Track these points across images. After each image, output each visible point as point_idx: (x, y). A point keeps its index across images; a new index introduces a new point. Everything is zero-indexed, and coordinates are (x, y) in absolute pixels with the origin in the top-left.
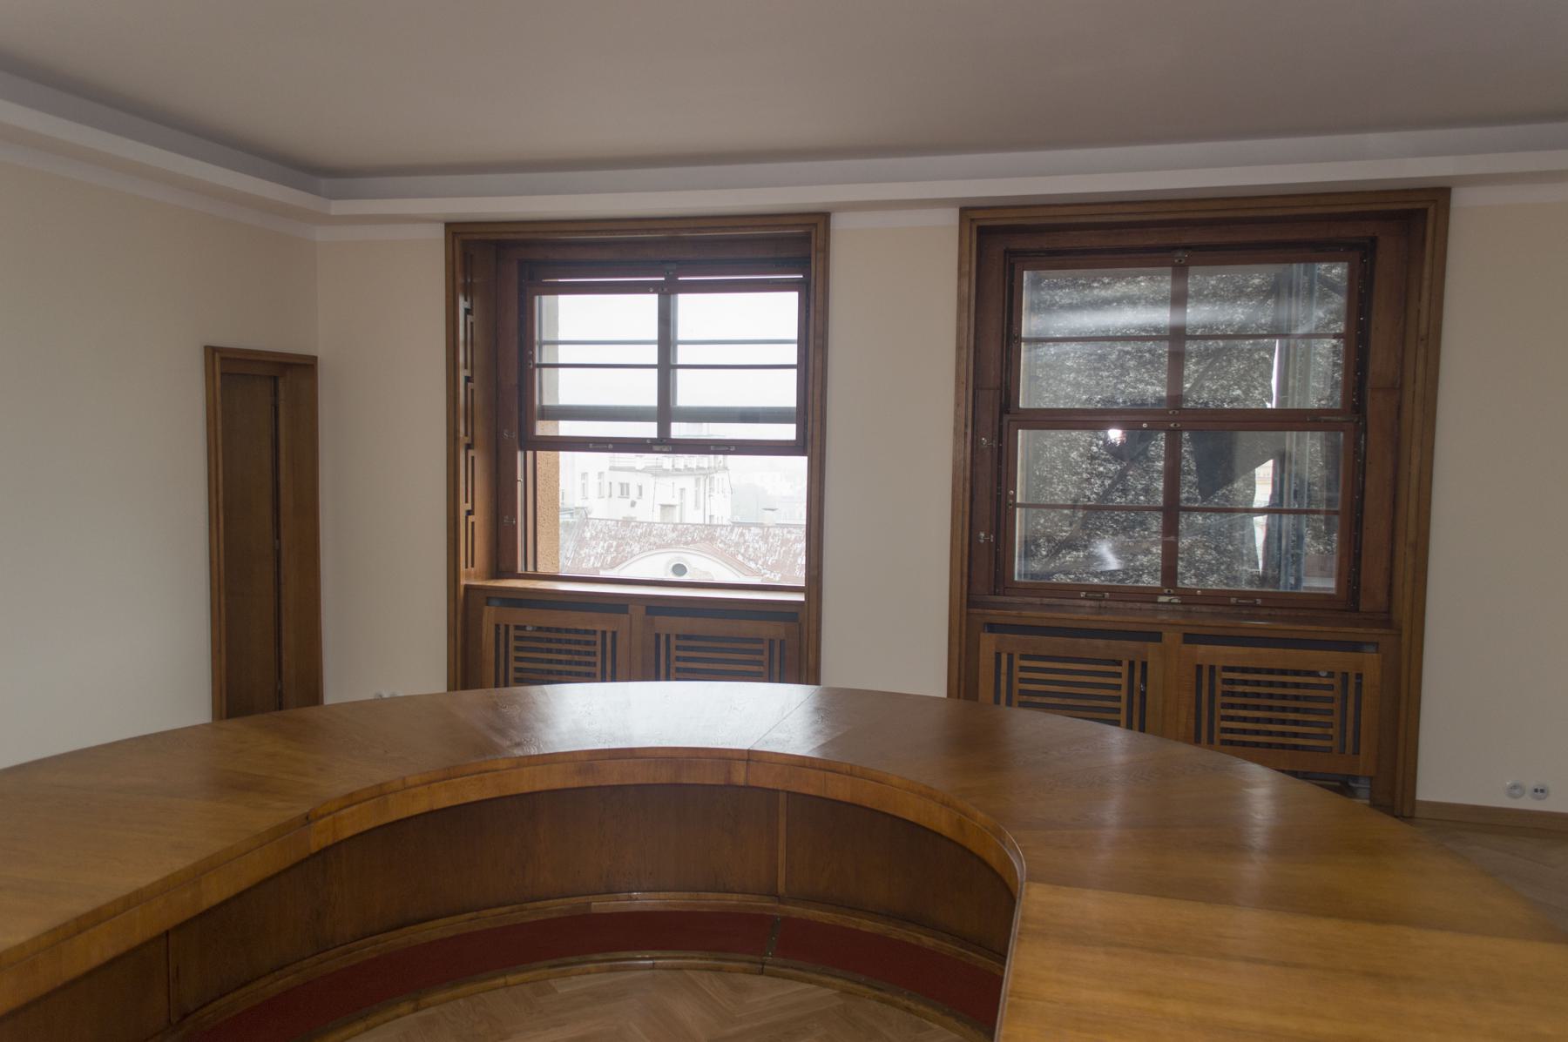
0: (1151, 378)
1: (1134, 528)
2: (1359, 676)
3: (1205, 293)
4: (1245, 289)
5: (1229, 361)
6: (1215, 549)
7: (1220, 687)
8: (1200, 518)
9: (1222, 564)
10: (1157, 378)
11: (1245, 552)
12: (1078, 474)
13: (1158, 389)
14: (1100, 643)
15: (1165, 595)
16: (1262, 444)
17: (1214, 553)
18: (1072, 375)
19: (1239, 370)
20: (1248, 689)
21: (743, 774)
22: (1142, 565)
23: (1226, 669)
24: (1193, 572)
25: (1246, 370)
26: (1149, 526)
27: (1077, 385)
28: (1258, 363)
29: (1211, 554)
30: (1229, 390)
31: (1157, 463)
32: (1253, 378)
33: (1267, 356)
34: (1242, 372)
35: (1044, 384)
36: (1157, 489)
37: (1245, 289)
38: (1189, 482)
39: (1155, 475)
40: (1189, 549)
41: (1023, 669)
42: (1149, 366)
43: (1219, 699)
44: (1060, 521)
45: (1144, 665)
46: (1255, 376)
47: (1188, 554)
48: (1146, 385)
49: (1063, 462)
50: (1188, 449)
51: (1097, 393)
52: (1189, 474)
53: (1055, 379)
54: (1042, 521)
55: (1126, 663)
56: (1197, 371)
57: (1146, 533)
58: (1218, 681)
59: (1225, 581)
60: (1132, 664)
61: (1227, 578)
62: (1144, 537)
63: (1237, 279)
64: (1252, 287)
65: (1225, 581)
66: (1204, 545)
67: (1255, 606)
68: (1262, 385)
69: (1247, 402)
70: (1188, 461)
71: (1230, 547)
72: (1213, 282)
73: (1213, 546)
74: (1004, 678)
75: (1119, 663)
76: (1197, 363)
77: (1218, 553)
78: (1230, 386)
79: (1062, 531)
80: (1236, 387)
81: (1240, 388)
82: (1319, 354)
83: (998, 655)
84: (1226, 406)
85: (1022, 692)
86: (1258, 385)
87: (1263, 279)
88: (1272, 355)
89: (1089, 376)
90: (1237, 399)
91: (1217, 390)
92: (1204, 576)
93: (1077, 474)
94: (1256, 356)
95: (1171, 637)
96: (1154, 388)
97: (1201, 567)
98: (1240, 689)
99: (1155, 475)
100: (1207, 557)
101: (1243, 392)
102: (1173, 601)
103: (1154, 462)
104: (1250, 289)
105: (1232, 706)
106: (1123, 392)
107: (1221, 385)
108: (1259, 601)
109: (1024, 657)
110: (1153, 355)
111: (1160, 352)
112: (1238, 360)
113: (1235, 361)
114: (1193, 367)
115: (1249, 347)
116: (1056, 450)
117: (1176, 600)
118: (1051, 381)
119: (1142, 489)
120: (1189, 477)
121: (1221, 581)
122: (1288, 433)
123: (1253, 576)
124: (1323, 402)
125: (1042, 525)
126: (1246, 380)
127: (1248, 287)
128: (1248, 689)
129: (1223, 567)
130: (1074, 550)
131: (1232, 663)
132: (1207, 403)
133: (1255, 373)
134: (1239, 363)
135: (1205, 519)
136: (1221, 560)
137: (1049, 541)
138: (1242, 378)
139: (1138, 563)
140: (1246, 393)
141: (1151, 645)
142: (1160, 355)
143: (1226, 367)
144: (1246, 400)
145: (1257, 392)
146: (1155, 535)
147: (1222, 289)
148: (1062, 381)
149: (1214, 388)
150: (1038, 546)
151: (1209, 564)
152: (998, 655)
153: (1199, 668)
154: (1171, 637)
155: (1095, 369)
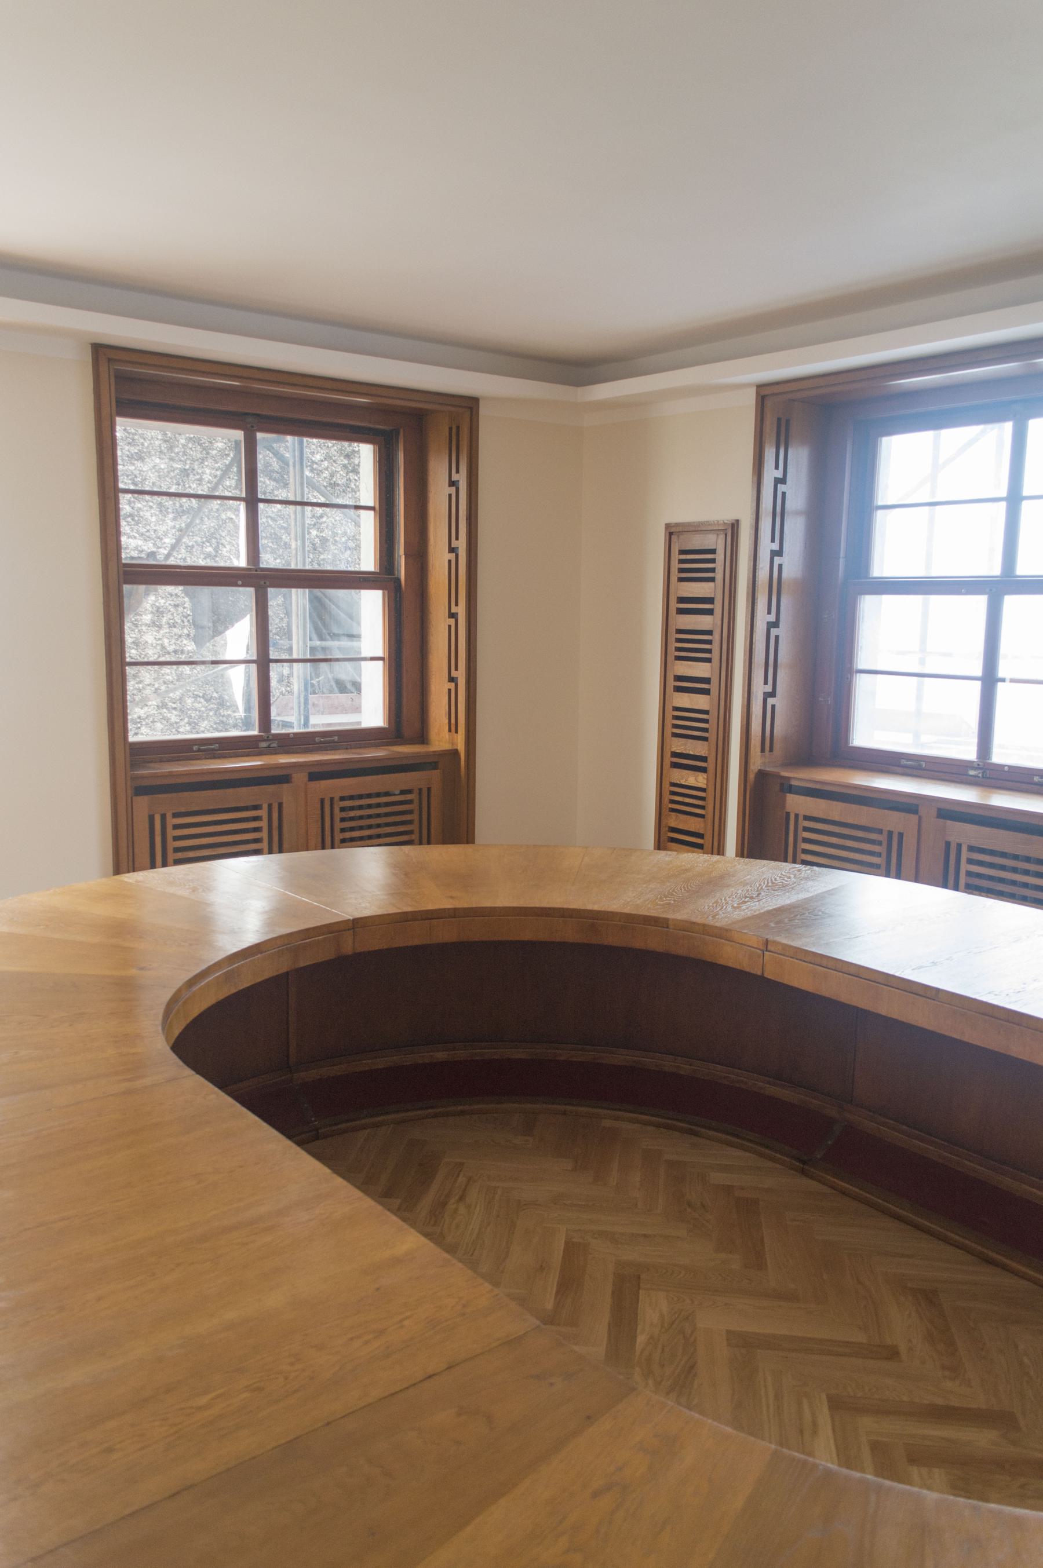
0: (132, 531)
2: (429, 789)
3: (176, 450)
4: (210, 451)
5: (202, 519)
6: (203, 697)
7: (338, 815)
8: (188, 669)
9: (210, 710)
10: (138, 532)
11: (226, 697)
13: (140, 543)
14: (243, 790)
15: (264, 740)
16: (244, 598)
17: (202, 700)
20: (358, 813)
21: (350, 942)
22: (139, 717)
23: (342, 799)
24: (186, 720)
25: (215, 529)
26: (142, 679)
28: (225, 522)
29: (200, 702)
30: (202, 547)
31: (144, 617)
32: (221, 536)
33: (234, 517)
34: (212, 530)
36: (147, 642)
37: (210, 451)
38: (175, 635)
39: (144, 628)
40: (181, 699)
41: (176, 827)
42: (129, 519)
43: (338, 825)
45: (280, 805)
46: (223, 534)
47: (180, 703)
48: (129, 538)
50: (172, 603)
52: (175, 627)
55: (265, 806)
56: (174, 527)
57: (141, 686)
58: (337, 810)
59: (215, 726)
60: (270, 806)
61: (216, 723)
62: (139, 690)
63: (203, 441)
64: (216, 449)
65: (215, 726)
66: (193, 694)
67: (334, 742)
68: (230, 543)
69: (217, 559)
70: (172, 614)
71: (215, 695)
72: (183, 441)
73: (201, 695)
74: (158, 839)
75: (256, 807)
76: (174, 519)
77: (207, 701)
78: (203, 543)
80: (208, 544)
81: (211, 545)
82: (269, 516)
83: (151, 818)
84: (201, 562)
85: (177, 850)
86: (226, 543)
87: (225, 443)
88: (238, 516)
90: (208, 556)
91: (193, 547)
92: (196, 724)
94: (224, 516)
95: (300, 778)
96: (135, 541)
97: (193, 715)
98: (352, 814)
99: (144, 628)
100: (197, 705)
101: (214, 549)
102: (272, 746)
103: (141, 615)
104: (214, 452)
105: (352, 829)
107: (196, 542)
108: (336, 738)
109: (175, 815)
110: (133, 508)
111: (139, 505)
112: (209, 519)
113: (206, 519)
114: (170, 524)
115: (217, 507)
117: (274, 745)
119: (133, 642)
120: (175, 629)
121: (211, 727)
122: (294, 590)
123: (236, 720)
124: (278, 561)
126: (216, 538)
127: (213, 449)
128: (358, 813)
129: (211, 713)
131: (346, 794)
132: (185, 559)
133: (223, 531)
134: (210, 521)
135: (191, 670)
136: (209, 707)
138: (212, 536)
139: (135, 716)
140: (216, 549)
141: (285, 786)
142: (140, 509)
143: (199, 524)
144: (216, 556)
145: (225, 549)
146: (149, 687)
147: (191, 449)
149: (190, 544)
151: (200, 711)
152: (151, 818)
153: (322, 801)
154: (300, 778)
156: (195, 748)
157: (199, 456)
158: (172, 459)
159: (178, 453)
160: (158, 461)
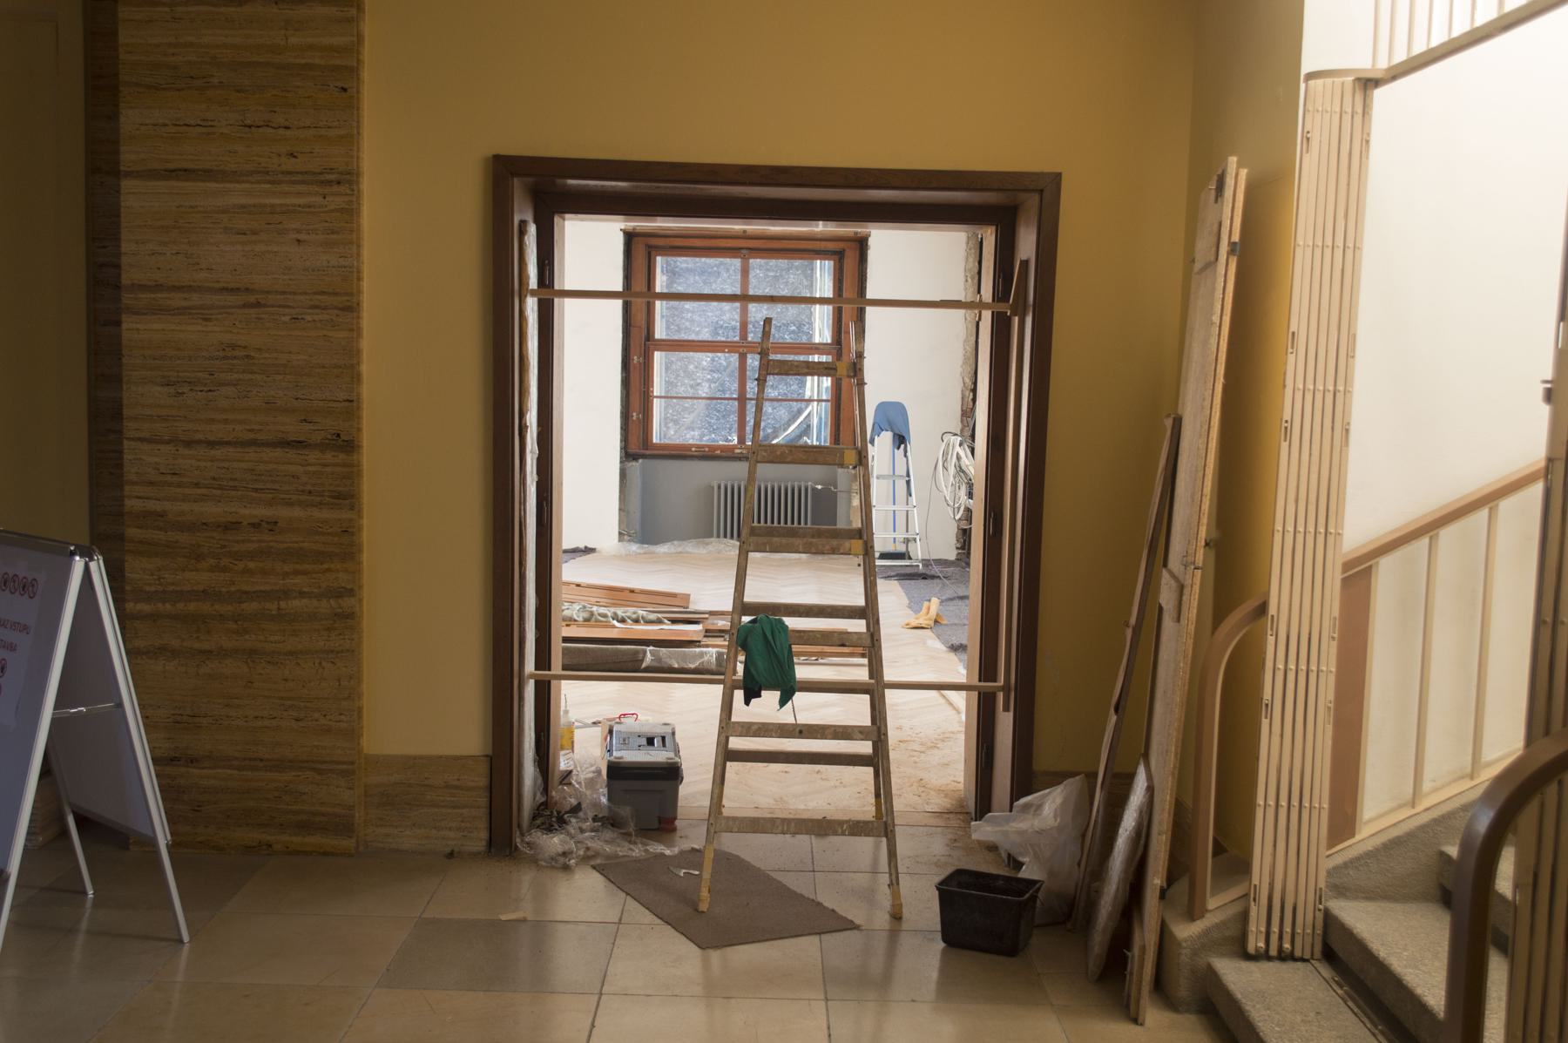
1: (729, 415)
12: (693, 380)
18: (690, 315)
19: (793, 314)
27: (692, 321)
35: (671, 320)
44: (683, 411)
49: (684, 372)
51: (706, 327)
53: (678, 316)
54: (671, 411)
79: (684, 418)
89: (700, 316)
90: (793, 332)
93: (693, 380)
106: (722, 327)
107: (783, 324)
116: (680, 364)
118: (675, 318)
125: (671, 414)
130: (693, 430)
137: (676, 425)
148: (683, 318)
150: (668, 428)
155: (704, 311)
156: (693, 449)
157: (787, 266)
158: (768, 270)
159: (771, 266)
160: (758, 272)
